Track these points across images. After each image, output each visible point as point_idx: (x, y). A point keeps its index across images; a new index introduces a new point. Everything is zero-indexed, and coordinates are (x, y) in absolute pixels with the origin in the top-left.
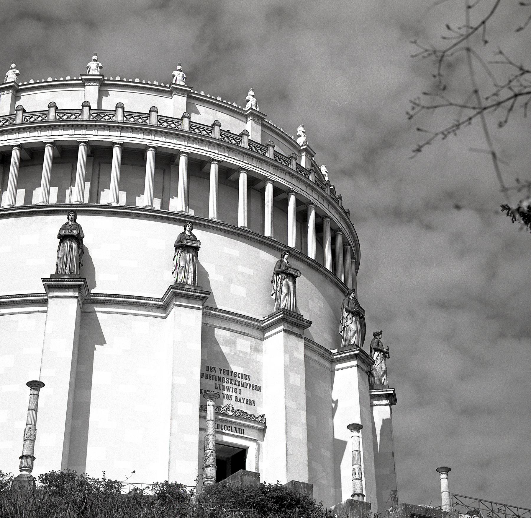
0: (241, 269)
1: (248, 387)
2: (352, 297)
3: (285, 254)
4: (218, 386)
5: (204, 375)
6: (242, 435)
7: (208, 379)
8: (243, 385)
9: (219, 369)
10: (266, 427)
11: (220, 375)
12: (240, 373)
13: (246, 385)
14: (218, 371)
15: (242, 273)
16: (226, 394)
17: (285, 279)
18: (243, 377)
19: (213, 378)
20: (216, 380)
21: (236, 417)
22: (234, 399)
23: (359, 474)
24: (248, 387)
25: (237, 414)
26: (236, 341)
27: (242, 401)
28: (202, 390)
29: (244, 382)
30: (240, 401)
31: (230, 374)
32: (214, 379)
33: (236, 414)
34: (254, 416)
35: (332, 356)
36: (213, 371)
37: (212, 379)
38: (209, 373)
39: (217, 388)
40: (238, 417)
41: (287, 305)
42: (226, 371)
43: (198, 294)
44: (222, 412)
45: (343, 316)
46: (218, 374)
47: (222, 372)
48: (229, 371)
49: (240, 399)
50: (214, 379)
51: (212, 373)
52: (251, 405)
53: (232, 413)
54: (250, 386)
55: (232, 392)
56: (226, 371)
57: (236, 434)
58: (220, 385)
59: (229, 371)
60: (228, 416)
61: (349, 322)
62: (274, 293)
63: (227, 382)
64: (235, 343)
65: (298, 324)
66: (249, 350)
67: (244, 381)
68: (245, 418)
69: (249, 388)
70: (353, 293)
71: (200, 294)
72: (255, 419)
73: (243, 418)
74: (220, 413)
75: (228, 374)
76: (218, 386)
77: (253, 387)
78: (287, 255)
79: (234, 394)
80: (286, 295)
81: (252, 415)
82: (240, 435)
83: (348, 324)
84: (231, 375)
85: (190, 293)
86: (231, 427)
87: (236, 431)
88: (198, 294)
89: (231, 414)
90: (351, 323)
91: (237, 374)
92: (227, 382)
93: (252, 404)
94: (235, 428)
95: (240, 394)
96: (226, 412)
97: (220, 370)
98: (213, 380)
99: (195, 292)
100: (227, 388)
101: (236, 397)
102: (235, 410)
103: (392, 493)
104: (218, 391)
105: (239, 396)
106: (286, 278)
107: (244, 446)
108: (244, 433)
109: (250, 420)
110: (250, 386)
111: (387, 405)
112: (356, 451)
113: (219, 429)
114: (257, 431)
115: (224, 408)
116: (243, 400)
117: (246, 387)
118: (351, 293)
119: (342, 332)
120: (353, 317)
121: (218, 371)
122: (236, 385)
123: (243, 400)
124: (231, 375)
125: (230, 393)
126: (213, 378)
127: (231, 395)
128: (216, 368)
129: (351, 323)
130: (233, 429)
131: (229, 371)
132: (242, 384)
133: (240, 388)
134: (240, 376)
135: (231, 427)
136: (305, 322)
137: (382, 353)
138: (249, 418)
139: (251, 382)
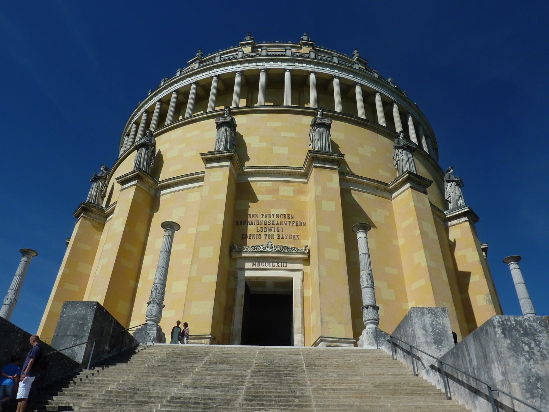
0: (283, 134)
2: (402, 138)
3: (318, 112)
4: (259, 229)
5: (246, 222)
8: (286, 224)
9: (261, 214)
10: (309, 257)
11: (261, 219)
13: (289, 223)
14: (260, 217)
15: (285, 137)
16: (268, 234)
17: (316, 129)
18: (286, 217)
19: (255, 223)
20: (258, 224)
21: (276, 252)
22: (276, 237)
23: (367, 281)
24: (292, 224)
25: (276, 249)
26: (278, 189)
27: (285, 237)
31: (272, 217)
32: (256, 224)
33: (275, 249)
34: (296, 248)
35: (388, 187)
36: (255, 217)
39: (258, 231)
40: (279, 252)
41: (319, 148)
42: (268, 215)
43: (224, 154)
44: (260, 250)
45: (395, 153)
46: (260, 218)
47: (264, 216)
48: (271, 214)
49: (283, 235)
50: (256, 224)
51: (254, 220)
52: (295, 239)
53: (271, 250)
54: (293, 223)
55: (275, 231)
56: (268, 215)
58: (262, 228)
59: (271, 215)
60: (267, 252)
61: (400, 155)
62: (311, 143)
63: (269, 224)
64: (277, 190)
65: (330, 159)
66: (292, 194)
67: (287, 220)
68: (286, 251)
70: (402, 134)
71: (226, 154)
72: (296, 250)
73: (284, 252)
74: (259, 252)
75: (270, 217)
76: (259, 229)
78: (320, 111)
79: (276, 233)
80: (318, 140)
81: (293, 248)
83: (399, 158)
85: (217, 155)
88: (224, 154)
89: (270, 251)
90: (402, 156)
92: (269, 224)
93: (296, 238)
96: (265, 249)
99: (222, 153)
100: (269, 229)
101: (279, 236)
102: (275, 246)
103: (486, 296)
104: (258, 233)
105: (281, 233)
106: (318, 128)
107: (292, 277)
108: (287, 266)
109: (291, 253)
110: (293, 223)
111: (466, 221)
112: (363, 254)
113: (259, 266)
114: (302, 262)
115: (262, 246)
116: (287, 237)
117: (289, 225)
118: (400, 135)
119: (396, 165)
120: (403, 151)
121: (260, 217)
123: (287, 237)
125: (272, 233)
126: (255, 223)
127: (273, 234)
128: (258, 214)
129: (402, 156)
131: (271, 215)
132: (284, 223)
133: (283, 226)
134: (283, 216)
136: (336, 156)
137: (454, 183)
138: (290, 251)
139: (295, 220)
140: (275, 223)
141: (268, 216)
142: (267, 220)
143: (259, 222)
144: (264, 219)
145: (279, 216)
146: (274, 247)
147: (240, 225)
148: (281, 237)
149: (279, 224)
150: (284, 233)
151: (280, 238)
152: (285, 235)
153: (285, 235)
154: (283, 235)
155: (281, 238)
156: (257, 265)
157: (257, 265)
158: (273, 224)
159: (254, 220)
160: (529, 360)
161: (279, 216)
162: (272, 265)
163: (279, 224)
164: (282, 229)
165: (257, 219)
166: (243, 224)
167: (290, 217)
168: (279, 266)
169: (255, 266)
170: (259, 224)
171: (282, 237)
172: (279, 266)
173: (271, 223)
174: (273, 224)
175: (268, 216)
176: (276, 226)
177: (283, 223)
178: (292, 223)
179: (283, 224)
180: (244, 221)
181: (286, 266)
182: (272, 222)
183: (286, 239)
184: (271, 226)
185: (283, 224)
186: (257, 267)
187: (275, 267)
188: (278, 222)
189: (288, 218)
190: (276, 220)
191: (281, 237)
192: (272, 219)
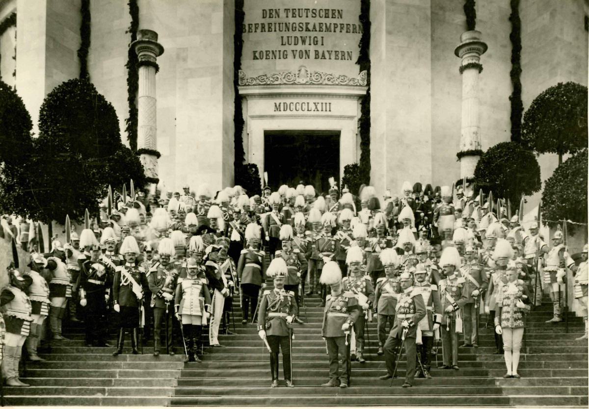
1: (338, 30)
4: (285, 40)
6: (328, 113)
7: (265, 31)
8: (328, 29)
11: (285, 20)
12: (324, 8)
13: (335, 28)
14: (282, 14)
22: (312, 55)
24: (338, 30)
28: (256, 51)
29: (331, 24)
30: (324, 57)
32: (277, 29)
37: (273, 30)
38: (267, 21)
47: (290, 14)
49: (323, 51)
50: (277, 29)
51: (273, 20)
54: (342, 28)
55: (310, 44)
57: (316, 113)
59: (303, 10)
63: (301, 29)
69: (341, 32)
76: (285, 40)
77: (348, 28)
79: (312, 48)
82: (324, 113)
84: (307, 17)
86: (308, 103)
87: (316, 108)
91: (318, 11)
95: (322, 45)
97: (287, 10)
98: (275, 31)
104: (282, 48)
116: (330, 55)
117: (335, 31)
122: (316, 31)
123: (330, 55)
124: (307, 17)
132: (326, 26)
134: (323, 14)
135: (308, 103)
140: (310, 27)
141: (297, 13)
142: (297, 20)
143: (284, 25)
144: (291, 20)
145: (317, 14)
146: (309, 75)
147: (249, 32)
148: (320, 55)
149: (318, 29)
150: (325, 49)
151: (318, 58)
152: (328, 51)
153: (328, 51)
154: (323, 51)
155: (320, 57)
158: (308, 30)
159: (273, 20)
161: (317, 14)
162: (306, 109)
163: (318, 29)
164: (321, 39)
165: (277, 20)
166: (254, 31)
167: (337, 14)
168: (318, 110)
169: (280, 111)
170: (284, 30)
171: (323, 56)
172: (318, 110)
173: (304, 28)
174: (308, 30)
175: (297, 13)
176: (313, 34)
177: (324, 27)
178: (339, 26)
179: (324, 30)
180: (256, 24)
182: (305, 25)
183: (330, 59)
185: (324, 30)
187: (312, 113)
188: (314, 26)
190: (312, 21)
191: (320, 55)
192: (304, 20)
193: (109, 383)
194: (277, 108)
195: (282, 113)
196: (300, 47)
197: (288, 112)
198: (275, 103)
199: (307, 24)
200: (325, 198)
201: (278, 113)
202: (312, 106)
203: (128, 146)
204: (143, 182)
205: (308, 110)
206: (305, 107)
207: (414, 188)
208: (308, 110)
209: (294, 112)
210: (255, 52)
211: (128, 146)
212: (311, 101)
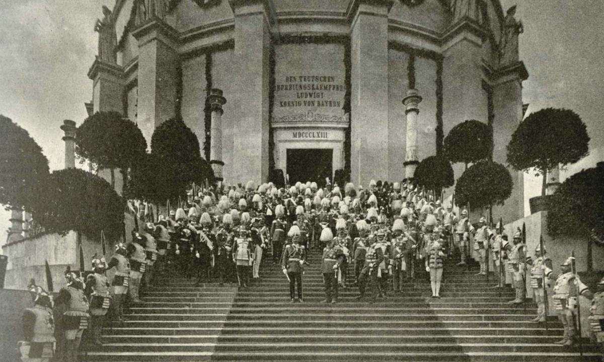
1: (332, 88)
4: (300, 95)
8: (326, 88)
14: (298, 79)
24: (332, 88)
30: (323, 105)
31: (311, 79)
38: (288, 84)
47: (303, 79)
54: (334, 88)
76: (300, 95)
94: (317, 133)
104: (298, 100)
130: (316, 135)
132: (324, 86)
140: (315, 87)
142: (307, 83)
144: (303, 83)
149: (319, 88)
153: (325, 102)
156: (298, 136)
157: (298, 136)
160: (405, 219)
163: (319, 88)
174: (313, 89)
176: (317, 91)
177: (323, 87)
181: (326, 137)
184: (311, 91)
186: (297, 139)
187: (315, 139)
189: (328, 81)
191: (321, 103)
193: (193, 301)
194: (295, 136)
195: (297, 139)
196: (308, 99)
197: (301, 138)
198: (294, 133)
199: (313, 85)
200: (323, 189)
201: (296, 139)
202: (316, 135)
203: (205, 159)
204: (214, 180)
205: (313, 137)
206: (311, 135)
207: (377, 183)
208: (313, 137)
209: (305, 138)
210: (281, 103)
211: (205, 159)
212: (315, 132)
